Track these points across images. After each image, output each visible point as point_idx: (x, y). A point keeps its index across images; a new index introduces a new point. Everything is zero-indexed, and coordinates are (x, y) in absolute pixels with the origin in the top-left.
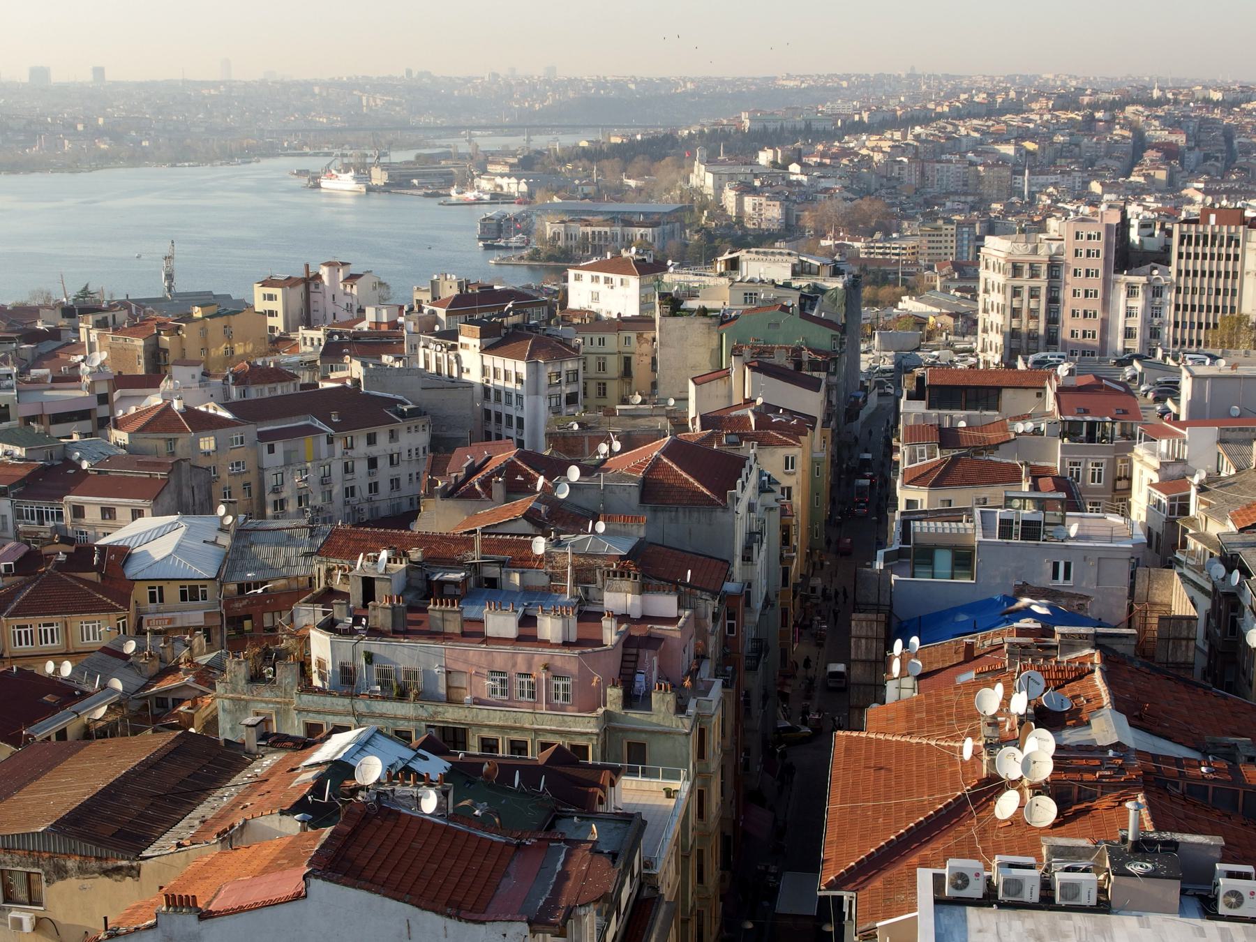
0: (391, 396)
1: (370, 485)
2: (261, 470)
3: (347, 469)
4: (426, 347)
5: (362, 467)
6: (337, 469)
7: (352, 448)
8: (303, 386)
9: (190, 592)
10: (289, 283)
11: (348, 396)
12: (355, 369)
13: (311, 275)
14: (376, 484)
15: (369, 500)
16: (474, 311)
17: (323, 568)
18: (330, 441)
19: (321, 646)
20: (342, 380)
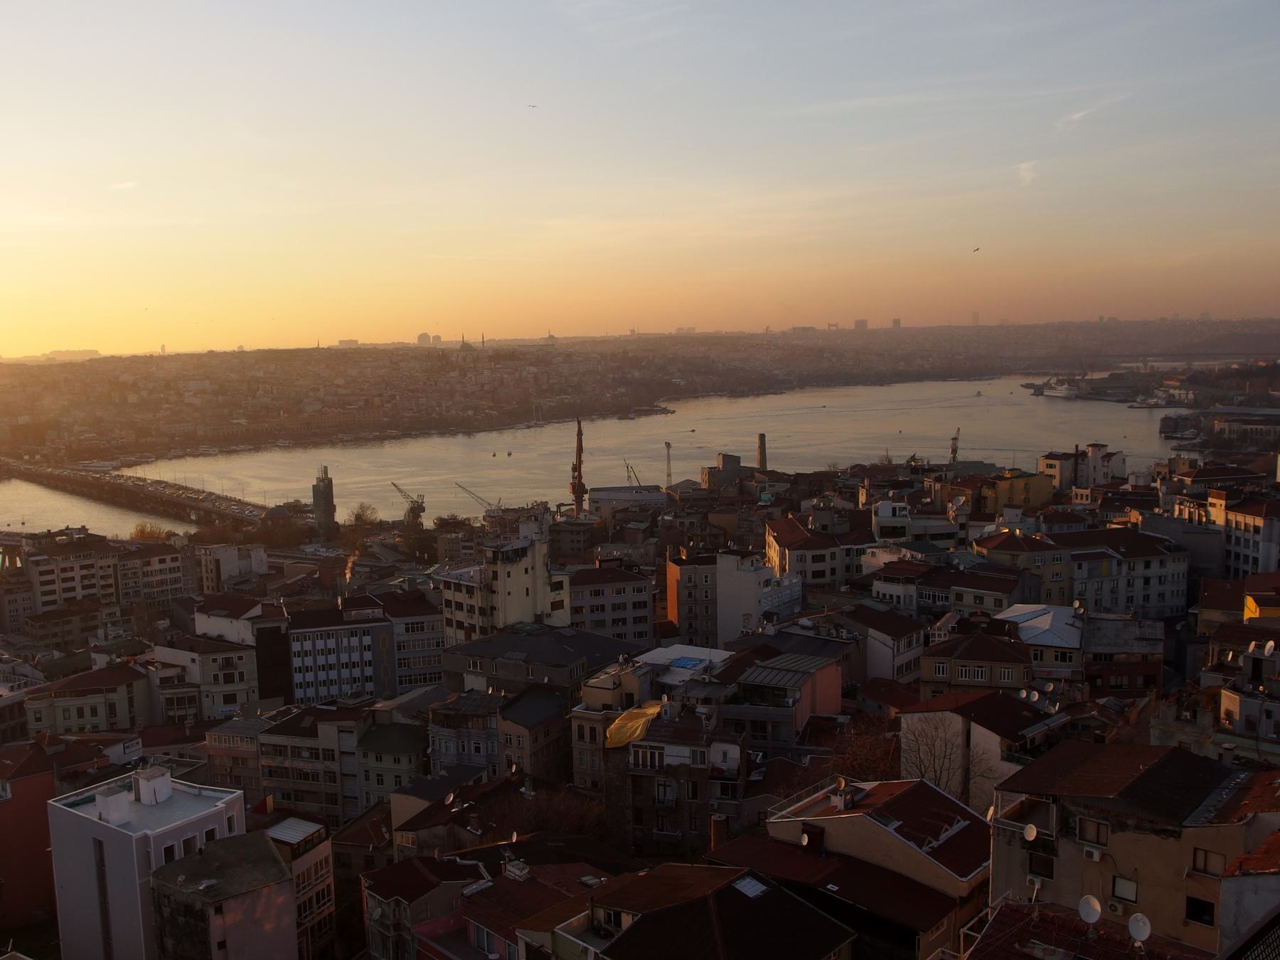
0: (1159, 536)
1: (1144, 596)
2: (1072, 579)
3: (1129, 584)
4: (1181, 504)
5: (1139, 583)
6: (1122, 583)
7: (1134, 569)
8: (1090, 527)
9: (1063, 655)
10: (1064, 457)
11: (1130, 537)
12: (1135, 516)
13: (1079, 452)
14: (1148, 595)
15: (1143, 606)
16: (1218, 481)
17: (1217, 649)
18: (1119, 564)
19: (1229, 701)
20: (1125, 523)
